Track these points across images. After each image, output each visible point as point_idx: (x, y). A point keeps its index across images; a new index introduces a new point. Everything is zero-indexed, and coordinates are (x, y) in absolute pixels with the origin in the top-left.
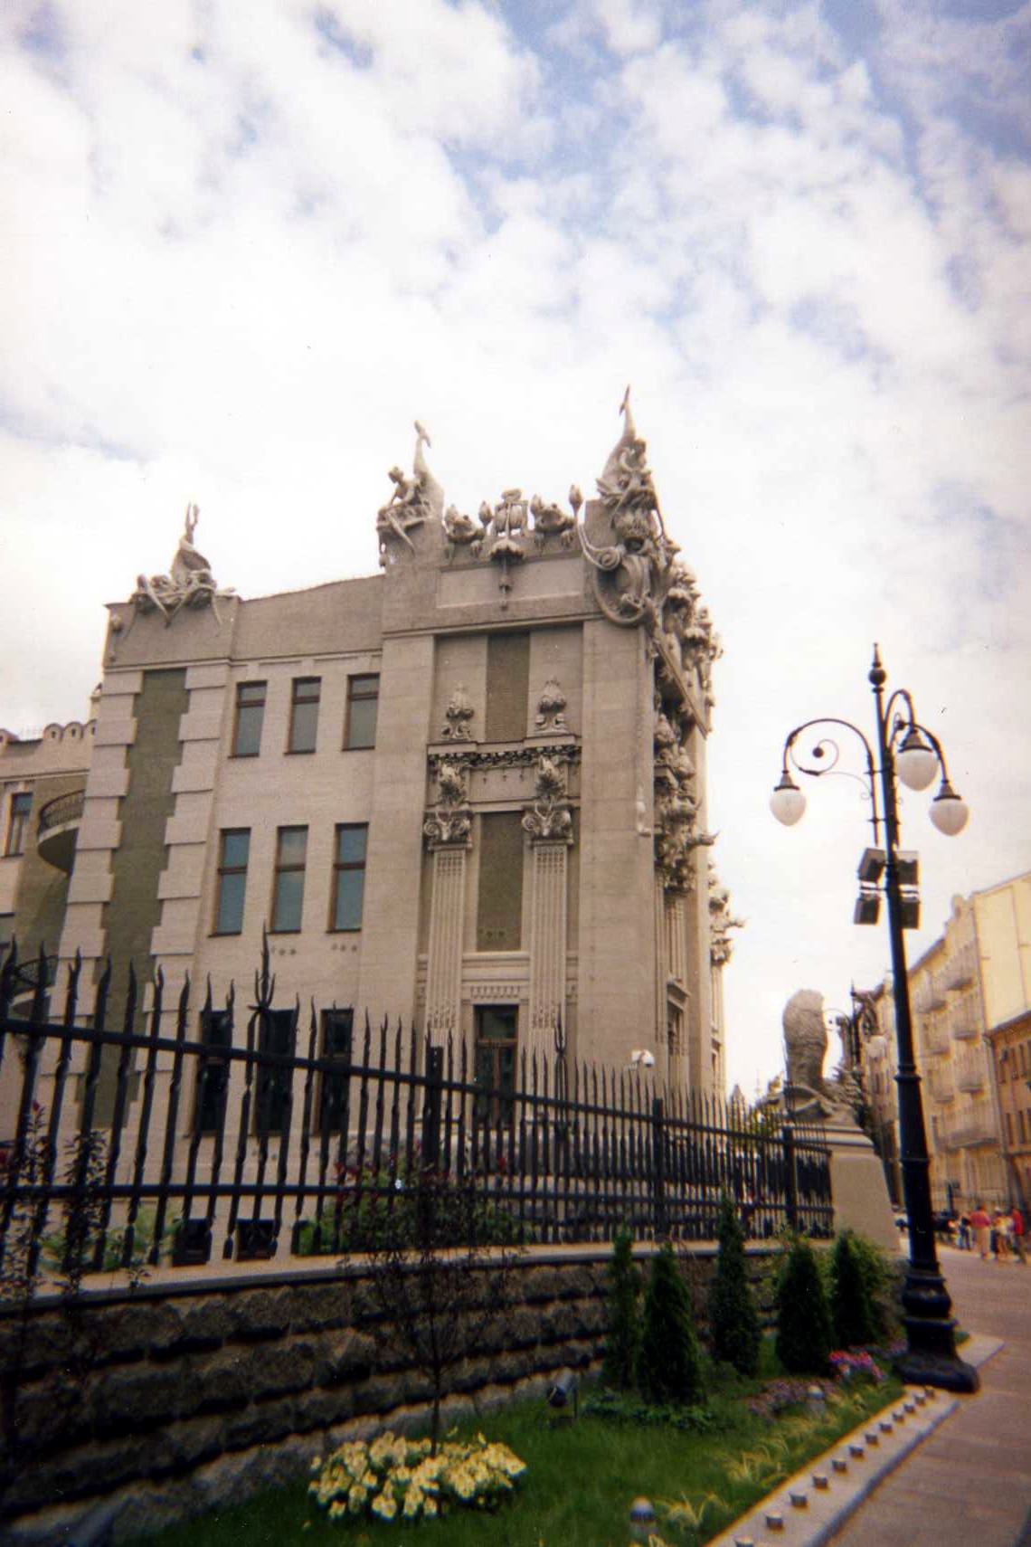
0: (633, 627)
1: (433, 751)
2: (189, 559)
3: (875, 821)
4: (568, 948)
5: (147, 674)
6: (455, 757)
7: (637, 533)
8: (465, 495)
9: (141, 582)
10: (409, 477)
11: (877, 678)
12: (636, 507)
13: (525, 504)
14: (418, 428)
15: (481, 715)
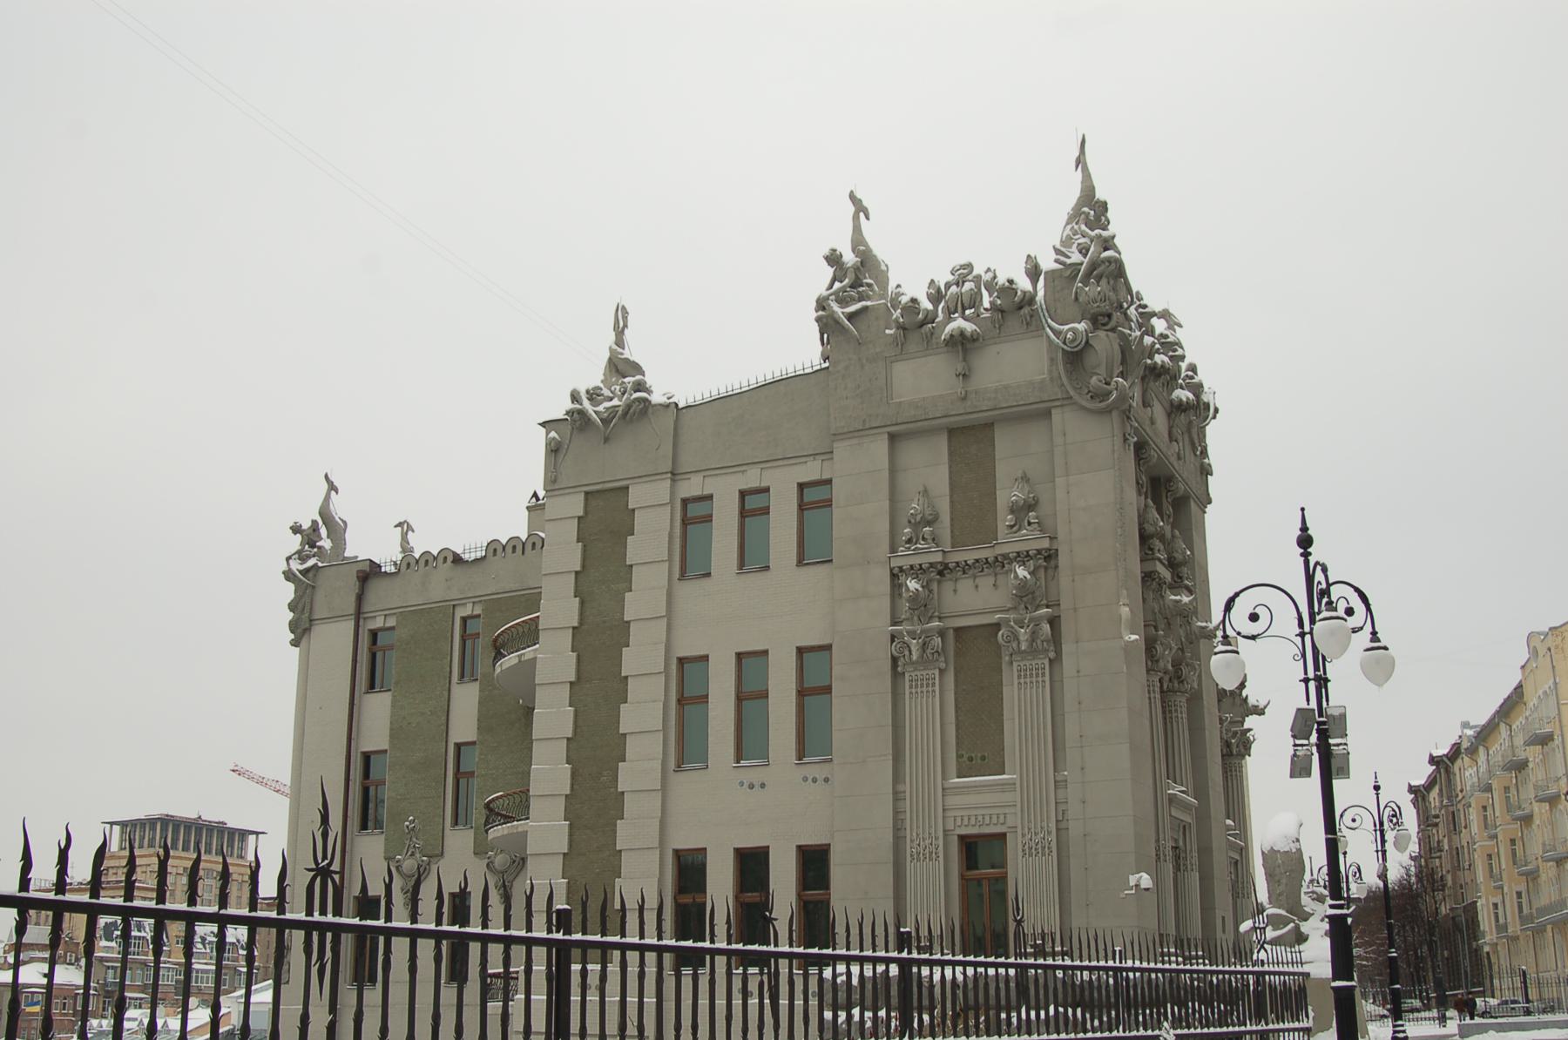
0: (1107, 411)
1: (896, 563)
2: (619, 367)
3: (1306, 681)
4: (1055, 770)
5: (587, 493)
6: (918, 587)
7: (1105, 307)
8: (912, 275)
9: (575, 397)
10: (849, 258)
11: (1305, 541)
12: (1099, 279)
13: (979, 277)
14: (852, 197)
15: (946, 518)
